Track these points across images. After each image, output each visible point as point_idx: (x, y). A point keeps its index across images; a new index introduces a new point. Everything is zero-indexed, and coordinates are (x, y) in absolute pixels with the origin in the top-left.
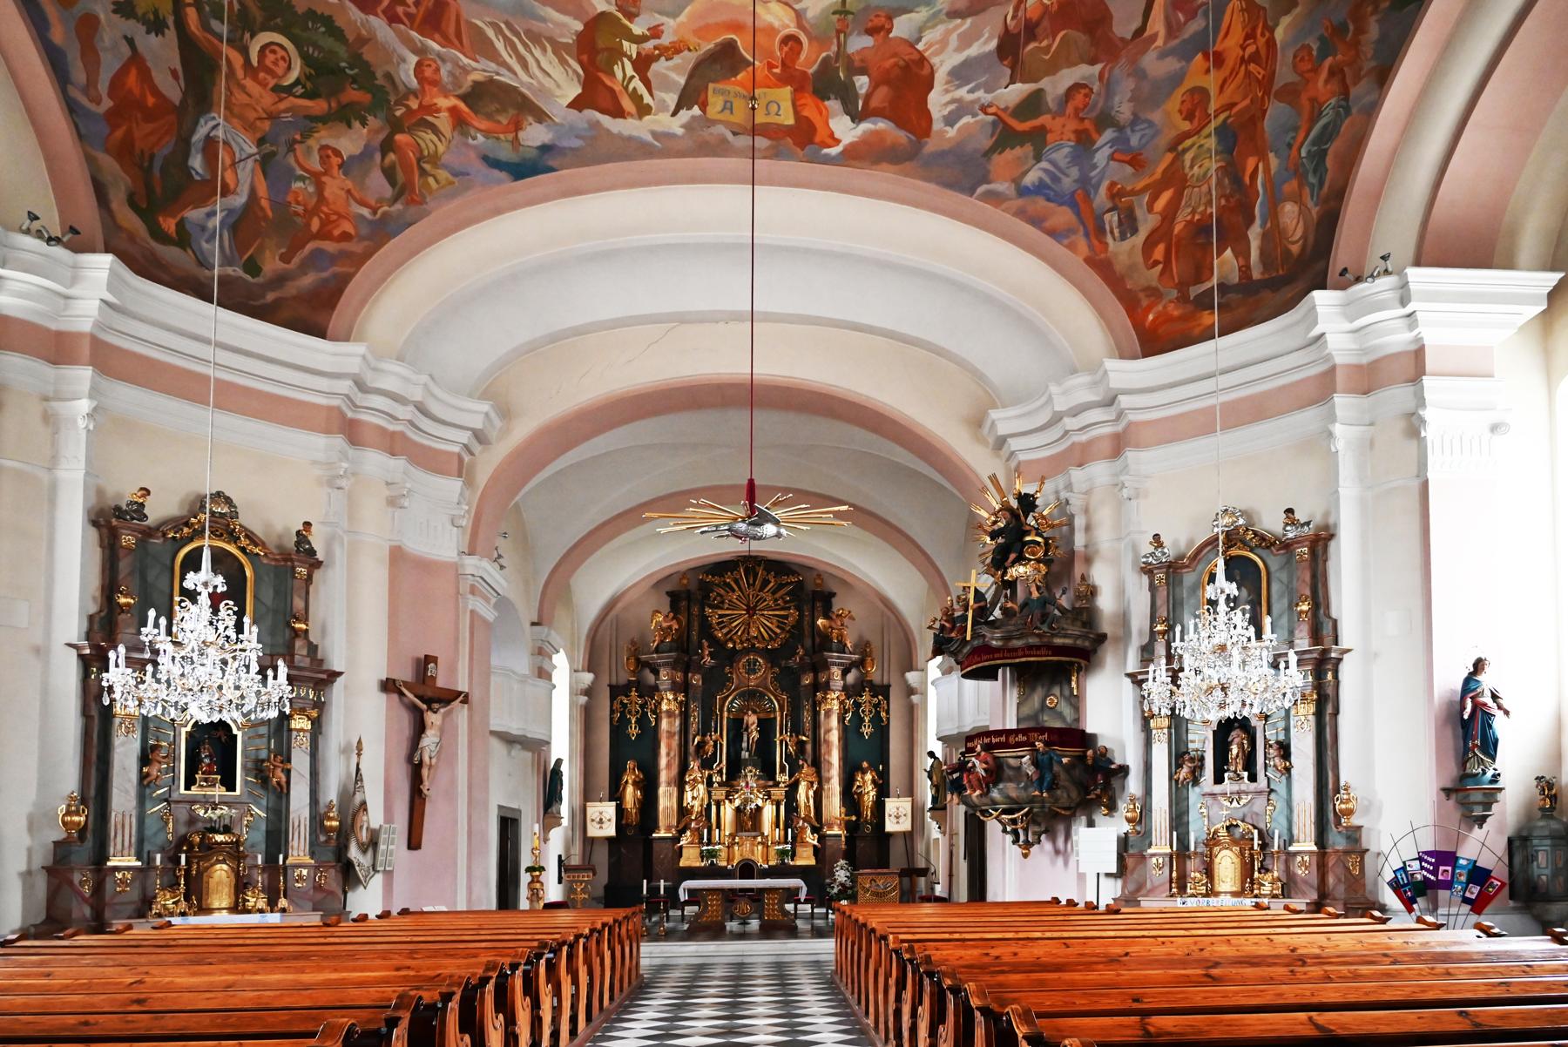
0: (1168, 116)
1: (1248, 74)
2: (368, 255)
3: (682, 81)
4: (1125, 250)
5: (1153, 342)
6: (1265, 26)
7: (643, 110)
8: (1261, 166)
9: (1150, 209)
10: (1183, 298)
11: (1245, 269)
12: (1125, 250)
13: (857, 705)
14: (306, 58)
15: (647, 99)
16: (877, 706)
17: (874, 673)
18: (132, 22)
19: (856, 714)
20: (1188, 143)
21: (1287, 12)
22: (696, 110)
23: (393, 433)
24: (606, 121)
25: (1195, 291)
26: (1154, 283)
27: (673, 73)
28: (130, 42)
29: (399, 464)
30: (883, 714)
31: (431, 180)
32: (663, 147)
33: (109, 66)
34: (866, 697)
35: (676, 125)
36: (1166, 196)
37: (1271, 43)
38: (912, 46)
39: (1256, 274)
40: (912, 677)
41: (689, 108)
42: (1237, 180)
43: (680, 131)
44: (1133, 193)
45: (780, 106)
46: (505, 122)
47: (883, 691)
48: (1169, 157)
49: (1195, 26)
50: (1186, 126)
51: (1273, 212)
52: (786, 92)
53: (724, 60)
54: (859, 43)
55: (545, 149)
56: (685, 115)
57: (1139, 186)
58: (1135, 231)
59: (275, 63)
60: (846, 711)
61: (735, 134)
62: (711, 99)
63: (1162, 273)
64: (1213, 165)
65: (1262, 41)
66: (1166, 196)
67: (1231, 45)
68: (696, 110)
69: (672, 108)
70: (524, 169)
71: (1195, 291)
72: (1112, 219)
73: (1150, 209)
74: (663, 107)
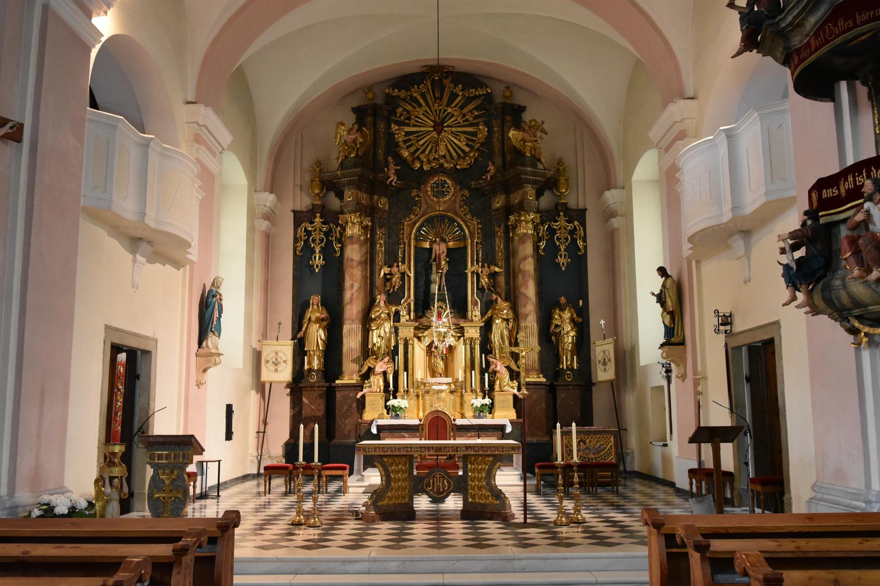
13: (552, 231)
16: (572, 232)
19: (551, 242)
60: (540, 239)
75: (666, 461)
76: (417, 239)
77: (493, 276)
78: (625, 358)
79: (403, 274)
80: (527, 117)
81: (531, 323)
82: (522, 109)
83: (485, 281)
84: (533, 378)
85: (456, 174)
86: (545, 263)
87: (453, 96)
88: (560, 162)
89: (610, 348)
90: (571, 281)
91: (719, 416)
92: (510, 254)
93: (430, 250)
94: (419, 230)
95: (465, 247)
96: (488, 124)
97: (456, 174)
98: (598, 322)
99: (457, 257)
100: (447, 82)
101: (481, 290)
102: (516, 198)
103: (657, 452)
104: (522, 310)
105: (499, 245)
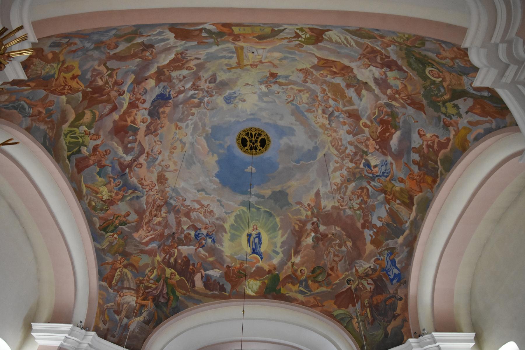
6: (69, 93)
8: (30, 88)
14: (425, 67)
18: (461, 113)
28: (467, 113)
33: (477, 118)
37: (63, 94)
59: (435, 74)
65: (66, 91)
67: (74, 84)
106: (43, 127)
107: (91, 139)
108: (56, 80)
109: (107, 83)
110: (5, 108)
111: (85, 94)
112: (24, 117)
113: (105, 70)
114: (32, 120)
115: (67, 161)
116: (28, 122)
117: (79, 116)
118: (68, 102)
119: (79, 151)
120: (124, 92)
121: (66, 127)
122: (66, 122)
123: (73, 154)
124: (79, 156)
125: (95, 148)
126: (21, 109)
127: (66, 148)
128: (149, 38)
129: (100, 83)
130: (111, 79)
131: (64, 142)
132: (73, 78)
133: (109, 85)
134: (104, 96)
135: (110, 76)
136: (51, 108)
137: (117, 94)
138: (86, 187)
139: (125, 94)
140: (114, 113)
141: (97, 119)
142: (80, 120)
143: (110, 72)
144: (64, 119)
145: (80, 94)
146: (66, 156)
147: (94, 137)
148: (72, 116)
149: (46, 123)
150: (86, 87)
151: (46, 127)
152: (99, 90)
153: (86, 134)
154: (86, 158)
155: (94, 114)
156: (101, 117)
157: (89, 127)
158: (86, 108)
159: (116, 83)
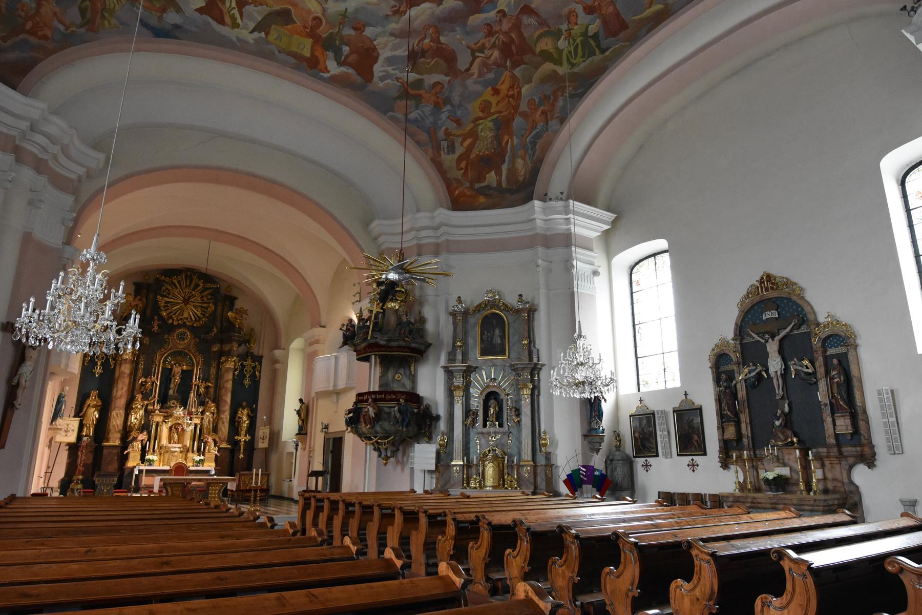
0: (474, 108)
1: (509, 102)
2: (55, 51)
3: (260, 19)
4: (449, 160)
5: (458, 204)
7: (235, 25)
9: (462, 145)
10: (472, 187)
11: (499, 182)
12: (449, 160)
13: (243, 366)
15: (239, 21)
16: (254, 368)
17: (255, 349)
19: (241, 372)
20: (481, 121)
21: (528, 83)
22: (263, 34)
23: (41, 159)
24: (214, 24)
25: (477, 186)
26: (460, 178)
27: (256, 13)
29: (43, 180)
30: (257, 373)
31: (106, 22)
32: (239, 47)
34: (249, 362)
35: (251, 38)
36: (468, 141)
37: (520, 93)
38: (371, 41)
39: (504, 185)
40: (278, 353)
41: (260, 32)
42: (500, 143)
43: (252, 42)
44: (454, 135)
45: (305, 47)
46: (158, 6)
47: (259, 359)
48: (472, 125)
49: (491, 76)
50: (481, 114)
51: (513, 162)
52: (309, 41)
53: (284, 17)
54: (348, 32)
55: (177, 27)
56: (256, 35)
57: (458, 133)
58: (454, 152)
60: (235, 370)
61: (279, 52)
62: (272, 31)
63: (464, 174)
64: (490, 134)
65: (516, 91)
66: (468, 141)
68: (263, 34)
69: (251, 29)
70: (162, 33)
71: (477, 186)
72: (444, 144)
73: (462, 145)
74: (246, 27)
75: (290, 488)
76: (164, 362)
77: (207, 388)
78: (275, 437)
79: (153, 383)
80: (238, 305)
81: (226, 416)
82: (236, 298)
83: (202, 390)
84: (224, 445)
85: (192, 329)
86: (238, 382)
87: (197, 285)
88: (252, 330)
89: (267, 431)
90: (252, 393)
91: (318, 466)
92: (219, 377)
93: (171, 369)
94: (166, 358)
95: (193, 371)
96: (215, 304)
97: (192, 329)
98: (262, 417)
99: (187, 376)
100: (195, 277)
101: (199, 395)
102: (227, 348)
103: (286, 484)
104: (222, 409)
105: (213, 371)
106: (560, 103)
107: (576, 24)
108: (501, 112)
109: (494, 46)
110: (533, 156)
111: (515, 65)
112: (547, 130)
113: (478, 60)
114: (552, 118)
115: (607, 53)
116: (553, 124)
117: (546, 56)
118: (529, 81)
119: (595, 37)
120: (498, 12)
121: (562, 70)
122: (555, 71)
123: (598, 46)
124: (602, 34)
125: (589, 10)
126: (538, 136)
127: (589, 60)
128: (400, 75)
129: (496, 54)
130: (487, 44)
131: (583, 65)
132: (496, 92)
133: (494, 43)
134: (511, 37)
135: (482, 49)
136: (537, 100)
137: (505, 21)
138: (650, 7)
139: (501, 8)
140: (533, 6)
141: (546, 29)
142: (550, 54)
143: (477, 54)
144: (553, 77)
145: (517, 72)
146: (601, 56)
147: (573, 18)
148: (548, 67)
149: (556, 100)
150: (506, 68)
151: (561, 98)
152: (506, 50)
153: (570, 35)
154: (605, 23)
155: (540, 37)
156: (542, 23)
157: (557, 35)
158: (533, 53)
159: (490, 33)
